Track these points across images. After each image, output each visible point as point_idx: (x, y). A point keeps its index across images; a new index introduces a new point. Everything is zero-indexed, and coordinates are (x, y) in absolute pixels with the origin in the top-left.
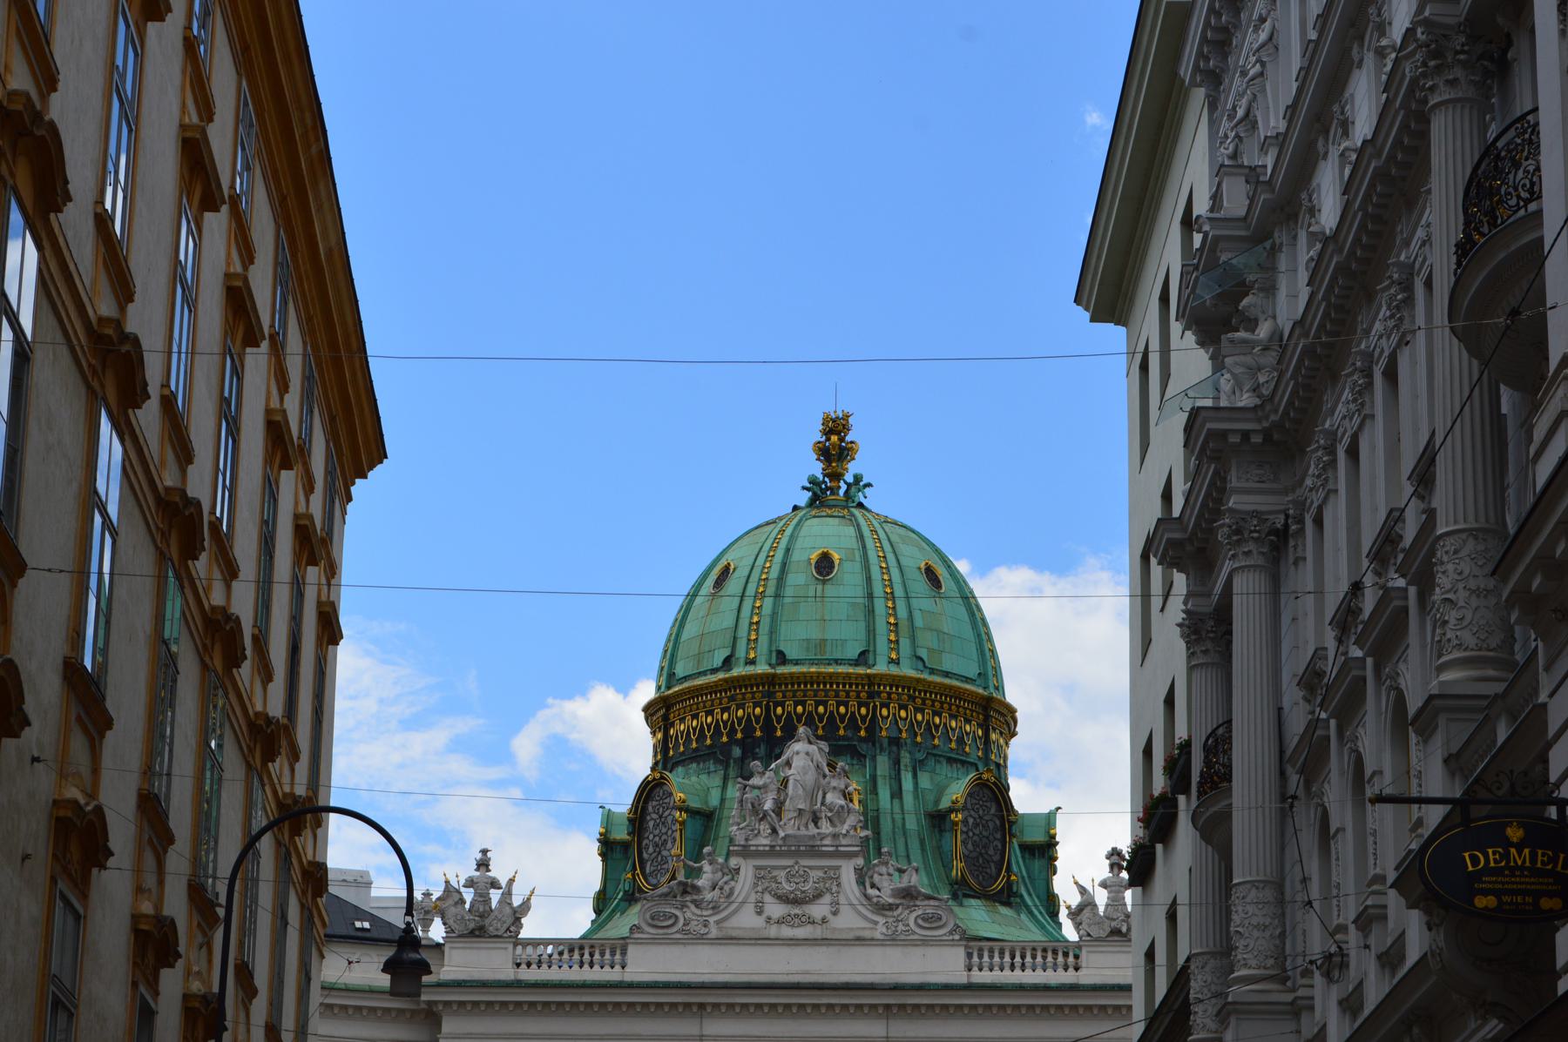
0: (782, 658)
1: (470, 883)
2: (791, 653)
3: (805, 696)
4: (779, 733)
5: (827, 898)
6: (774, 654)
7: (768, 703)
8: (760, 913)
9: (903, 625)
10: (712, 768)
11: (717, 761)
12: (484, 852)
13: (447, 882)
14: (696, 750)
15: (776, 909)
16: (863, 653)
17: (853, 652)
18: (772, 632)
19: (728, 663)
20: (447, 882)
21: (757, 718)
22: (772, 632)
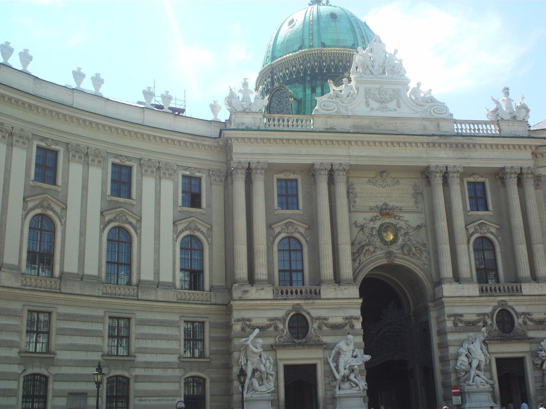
0: (323, 45)
1: (240, 91)
2: (327, 43)
3: (334, 58)
4: (325, 71)
5: (395, 101)
6: (320, 44)
7: (320, 60)
8: (368, 106)
9: (365, 37)
10: (297, 85)
11: (299, 83)
12: (245, 79)
13: (231, 90)
14: (289, 80)
15: (374, 104)
16: (353, 45)
17: (350, 43)
18: (319, 36)
19: (300, 48)
20: (231, 90)
21: (316, 66)
22: (319, 36)
